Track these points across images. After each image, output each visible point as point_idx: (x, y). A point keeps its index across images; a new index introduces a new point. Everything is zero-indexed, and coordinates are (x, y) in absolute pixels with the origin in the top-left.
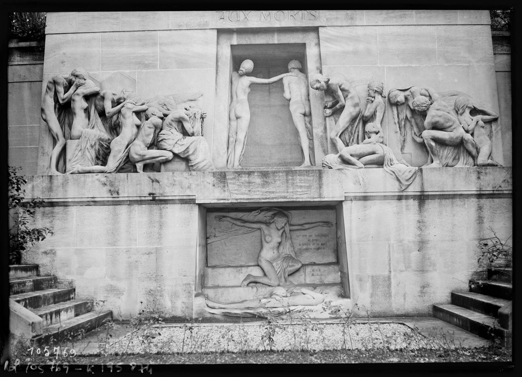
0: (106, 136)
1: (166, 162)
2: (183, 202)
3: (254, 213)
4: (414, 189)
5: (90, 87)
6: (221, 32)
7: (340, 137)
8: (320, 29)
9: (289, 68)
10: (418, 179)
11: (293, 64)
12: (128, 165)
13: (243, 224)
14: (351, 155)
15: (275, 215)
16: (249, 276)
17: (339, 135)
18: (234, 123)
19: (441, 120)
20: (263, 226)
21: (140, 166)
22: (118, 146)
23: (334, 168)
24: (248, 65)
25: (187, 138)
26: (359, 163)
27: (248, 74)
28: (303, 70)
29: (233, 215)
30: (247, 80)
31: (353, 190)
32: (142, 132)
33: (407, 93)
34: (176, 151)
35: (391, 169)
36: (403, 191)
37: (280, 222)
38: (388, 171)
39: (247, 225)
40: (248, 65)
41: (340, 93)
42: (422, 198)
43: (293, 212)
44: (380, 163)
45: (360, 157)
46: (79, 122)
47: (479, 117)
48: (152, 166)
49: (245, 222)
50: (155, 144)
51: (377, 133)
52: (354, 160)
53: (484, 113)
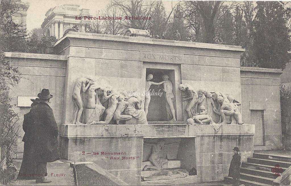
0: (104, 108)
2: (138, 137)
4: (219, 133)
5: (96, 86)
6: (144, 62)
8: (181, 65)
10: (221, 130)
12: (114, 121)
16: (146, 166)
19: (228, 106)
21: (118, 122)
22: (110, 112)
24: (151, 77)
25: (138, 110)
27: (151, 80)
30: (150, 83)
31: (200, 133)
32: (120, 106)
33: (214, 94)
34: (134, 116)
45: (202, 120)
46: (92, 100)
47: (236, 104)
48: (123, 122)
52: (200, 121)
53: (237, 102)
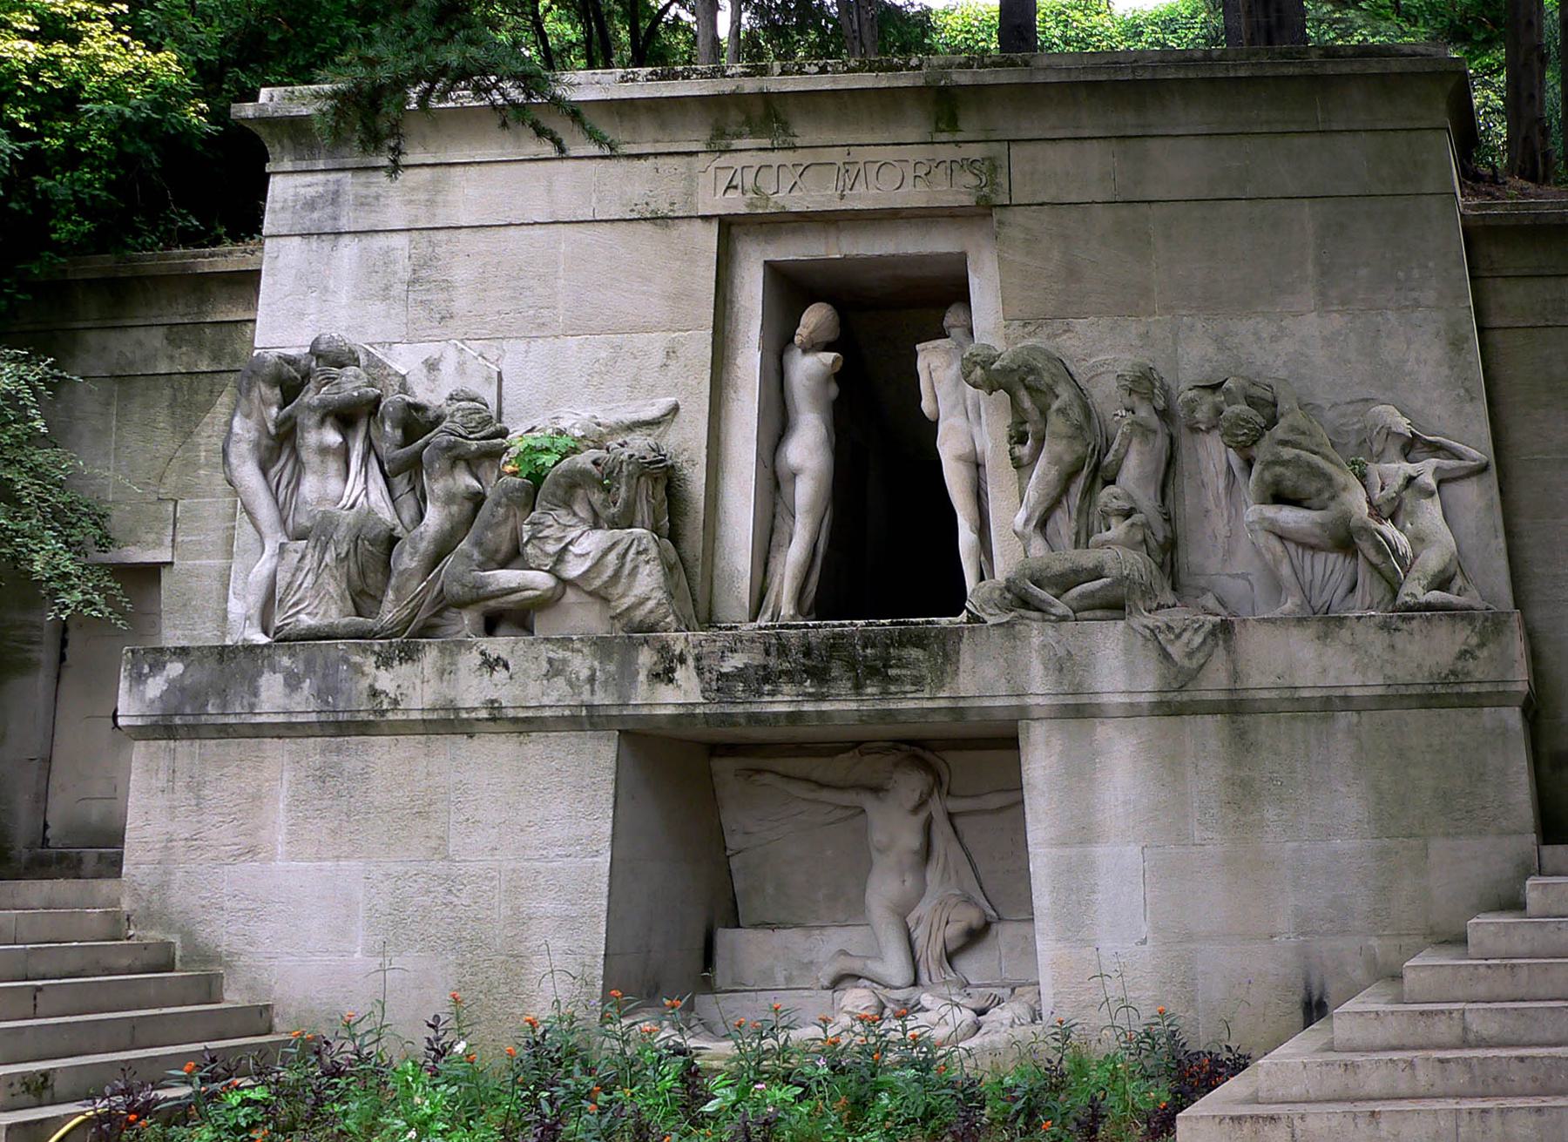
1: (546, 603)
3: (843, 760)
4: (1215, 682)
13: (811, 796)
14: (1037, 583)
15: (896, 765)
20: (868, 801)
23: (991, 621)
26: (1060, 608)
29: (782, 764)
35: (1145, 622)
36: (1180, 689)
37: (910, 785)
38: (1141, 629)
39: (825, 795)
42: (1235, 707)
43: (953, 757)
44: (1114, 607)
45: (1064, 582)
49: (822, 785)
50: (514, 557)
51: (1127, 514)
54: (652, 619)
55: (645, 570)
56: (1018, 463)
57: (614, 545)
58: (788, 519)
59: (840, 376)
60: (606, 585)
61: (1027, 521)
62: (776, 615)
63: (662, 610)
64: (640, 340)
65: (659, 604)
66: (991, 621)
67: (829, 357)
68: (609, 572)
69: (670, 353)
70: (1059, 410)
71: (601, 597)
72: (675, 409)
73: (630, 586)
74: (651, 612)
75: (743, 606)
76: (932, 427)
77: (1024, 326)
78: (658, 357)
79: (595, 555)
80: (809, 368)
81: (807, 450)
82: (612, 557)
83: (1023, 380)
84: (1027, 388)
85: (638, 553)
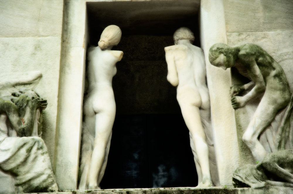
7: (259, 138)
9: (176, 38)
11: (183, 35)
14: (282, 165)
17: (257, 136)
18: (89, 120)
23: (253, 186)
24: (111, 33)
28: (197, 41)
40: (111, 33)
41: (257, 70)
54: (44, 185)
55: (41, 158)
56: (237, 106)
57: (25, 144)
58: (91, 137)
59: (119, 65)
60: (18, 166)
61: (254, 134)
62: (87, 186)
63: (50, 180)
64: (20, 40)
65: (49, 176)
66: (253, 186)
67: (118, 54)
68: (21, 159)
69: (37, 47)
70: (276, 76)
71: (13, 173)
72: (40, 77)
73: (32, 167)
74: (44, 181)
75: (72, 181)
76: (173, 90)
77: (239, 35)
78: (30, 49)
79: (13, 150)
80: (106, 60)
81: (104, 101)
82: (23, 151)
83: (257, 60)
84: (259, 64)
85: (38, 149)
